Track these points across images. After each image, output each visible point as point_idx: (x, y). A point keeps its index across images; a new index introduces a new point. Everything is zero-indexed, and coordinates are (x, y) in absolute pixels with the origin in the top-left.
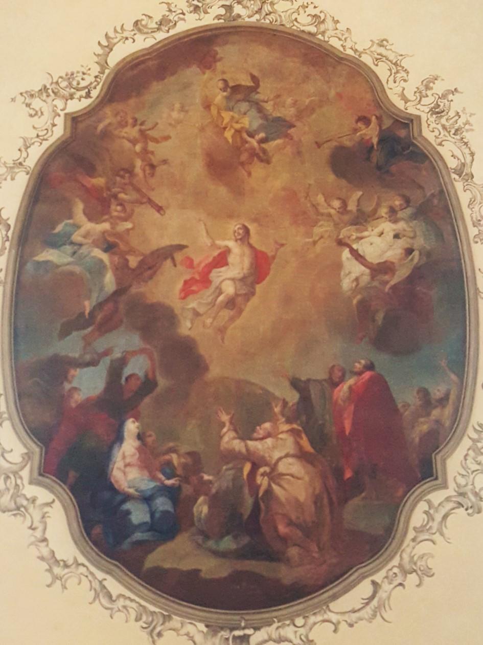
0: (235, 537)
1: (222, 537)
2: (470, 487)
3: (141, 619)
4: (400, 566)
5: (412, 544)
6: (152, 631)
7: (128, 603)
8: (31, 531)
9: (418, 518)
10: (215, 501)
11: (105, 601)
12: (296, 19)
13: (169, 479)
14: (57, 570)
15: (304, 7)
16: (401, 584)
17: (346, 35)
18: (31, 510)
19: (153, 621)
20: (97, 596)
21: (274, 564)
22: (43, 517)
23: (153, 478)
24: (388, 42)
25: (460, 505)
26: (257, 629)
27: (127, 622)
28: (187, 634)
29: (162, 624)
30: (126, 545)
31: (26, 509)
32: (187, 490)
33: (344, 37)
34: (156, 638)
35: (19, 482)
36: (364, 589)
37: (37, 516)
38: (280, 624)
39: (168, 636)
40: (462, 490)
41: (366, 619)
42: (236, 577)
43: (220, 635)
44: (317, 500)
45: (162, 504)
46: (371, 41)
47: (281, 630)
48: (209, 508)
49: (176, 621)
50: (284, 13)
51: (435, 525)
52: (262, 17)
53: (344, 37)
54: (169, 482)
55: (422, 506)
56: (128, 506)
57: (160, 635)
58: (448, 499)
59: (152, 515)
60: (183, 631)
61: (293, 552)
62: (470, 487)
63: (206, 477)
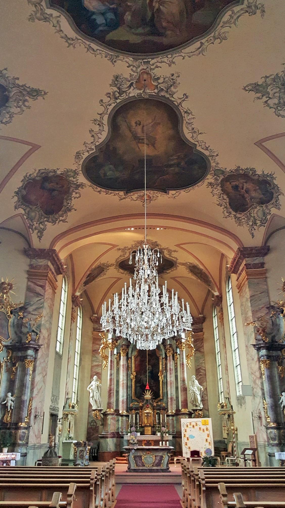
0: (144, 28)
1: (137, 28)
2: (254, 3)
4: (214, 37)
5: (220, 28)
7: (101, 52)
8: (54, 28)
9: (226, 18)
10: (134, 15)
11: (92, 52)
13: (111, 5)
14: (69, 41)
16: (212, 43)
18: (51, 19)
20: (88, 50)
21: (160, 38)
22: (58, 22)
23: (104, 5)
25: (247, 11)
26: (152, 59)
28: (126, 61)
30: (96, 32)
31: (50, 19)
32: (120, 9)
35: (42, 7)
36: (198, 44)
37: (55, 22)
40: (250, 5)
42: (145, 42)
44: (181, 13)
45: (110, 16)
48: (131, 17)
51: (233, 21)
54: (112, 6)
55: (230, 13)
56: (94, 17)
57: (115, 62)
58: (242, 9)
59: (106, 20)
61: (169, 32)
62: (254, 3)
63: (129, 4)
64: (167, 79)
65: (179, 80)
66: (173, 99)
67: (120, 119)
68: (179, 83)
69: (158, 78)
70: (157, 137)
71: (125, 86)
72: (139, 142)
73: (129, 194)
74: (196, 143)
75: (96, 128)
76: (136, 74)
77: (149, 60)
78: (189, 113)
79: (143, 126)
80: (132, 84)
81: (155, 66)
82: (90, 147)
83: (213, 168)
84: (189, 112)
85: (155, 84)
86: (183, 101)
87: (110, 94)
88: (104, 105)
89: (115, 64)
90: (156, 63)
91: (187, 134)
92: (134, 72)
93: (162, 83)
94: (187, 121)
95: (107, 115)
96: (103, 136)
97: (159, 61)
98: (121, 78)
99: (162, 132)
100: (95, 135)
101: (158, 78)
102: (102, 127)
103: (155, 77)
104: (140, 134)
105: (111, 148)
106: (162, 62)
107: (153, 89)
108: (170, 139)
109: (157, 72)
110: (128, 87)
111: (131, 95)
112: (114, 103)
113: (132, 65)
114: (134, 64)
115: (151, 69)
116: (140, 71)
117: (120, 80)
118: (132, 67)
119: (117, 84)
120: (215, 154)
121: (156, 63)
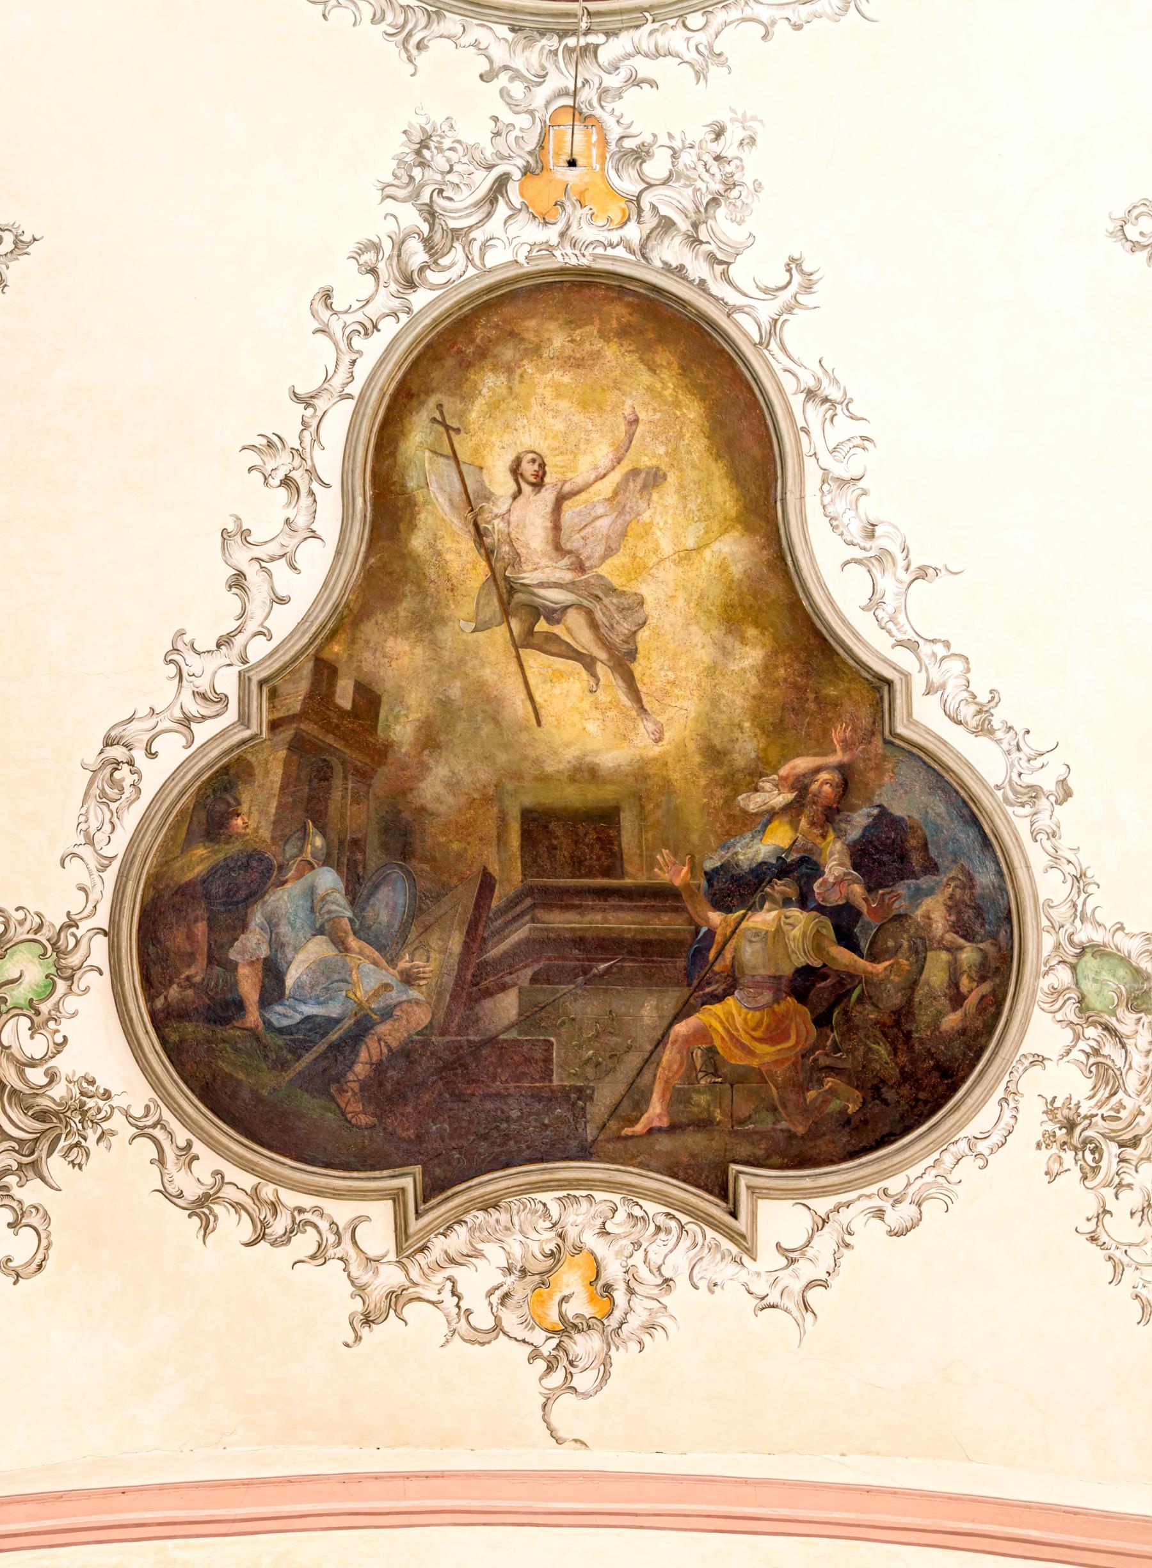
3: (383, 19)
6: (406, 40)
19: (406, 21)
26: (608, 34)
27: (354, 24)
28: (476, 44)
29: (425, 27)
34: (414, 52)
38: (656, 25)
39: (437, 47)
41: (828, 17)
43: (539, 45)
47: (658, 34)
49: (452, 23)
57: (420, 46)
60: (468, 39)
64: (687, 158)
65: (753, 166)
66: (733, 298)
67: (418, 436)
68: (758, 187)
69: (640, 155)
70: (646, 590)
71: (465, 198)
72: (528, 640)
73: (439, 1245)
74: (904, 659)
75: (268, 511)
76: (523, 121)
77: (592, 39)
78: (834, 404)
79: (560, 500)
80: (502, 183)
81: (623, 73)
82: (203, 685)
83: (1055, 928)
84: (835, 394)
85: (629, 184)
86: (789, 309)
87: (377, 247)
88: (336, 326)
89: (421, 59)
90: (629, 56)
91: (842, 591)
92: (513, 105)
93: (665, 182)
94: (826, 460)
95: (350, 405)
96: (308, 581)
97: (644, 47)
98: (447, 143)
99: (676, 556)
100: (252, 573)
101: (640, 155)
102: (305, 500)
103: (629, 144)
104: (541, 571)
105: (344, 695)
106: (657, 54)
107: (617, 218)
108: (737, 612)
109: (636, 115)
110: (478, 204)
111: (493, 258)
112: (394, 314)
113: (506, 68)
114: (519, 63)
115: (603, 93)
116: (548, 104)
117: (440, 162)
118: (504, 77)
119: (422, 186)
120: (1047, 781)
121: (629, 56)
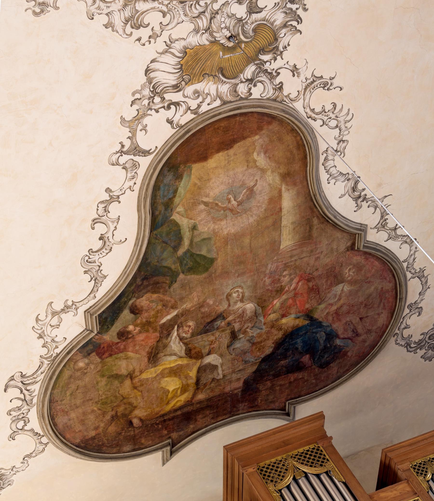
12: (164, 16)
15: (153, 37)
17: (93, 9)
24: (34, 12)
33: (96, 5)
46: (57, 8)
50: (180, 20)
52: (210, 7)
53: (96, 5)
